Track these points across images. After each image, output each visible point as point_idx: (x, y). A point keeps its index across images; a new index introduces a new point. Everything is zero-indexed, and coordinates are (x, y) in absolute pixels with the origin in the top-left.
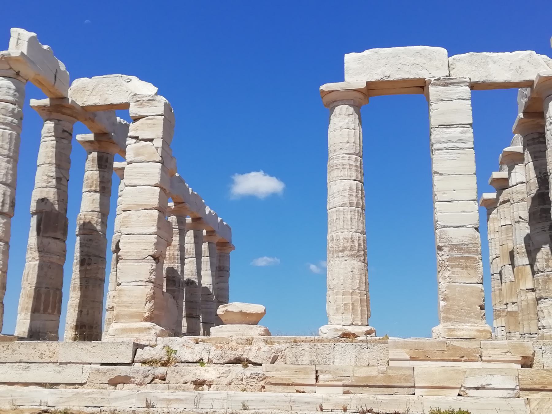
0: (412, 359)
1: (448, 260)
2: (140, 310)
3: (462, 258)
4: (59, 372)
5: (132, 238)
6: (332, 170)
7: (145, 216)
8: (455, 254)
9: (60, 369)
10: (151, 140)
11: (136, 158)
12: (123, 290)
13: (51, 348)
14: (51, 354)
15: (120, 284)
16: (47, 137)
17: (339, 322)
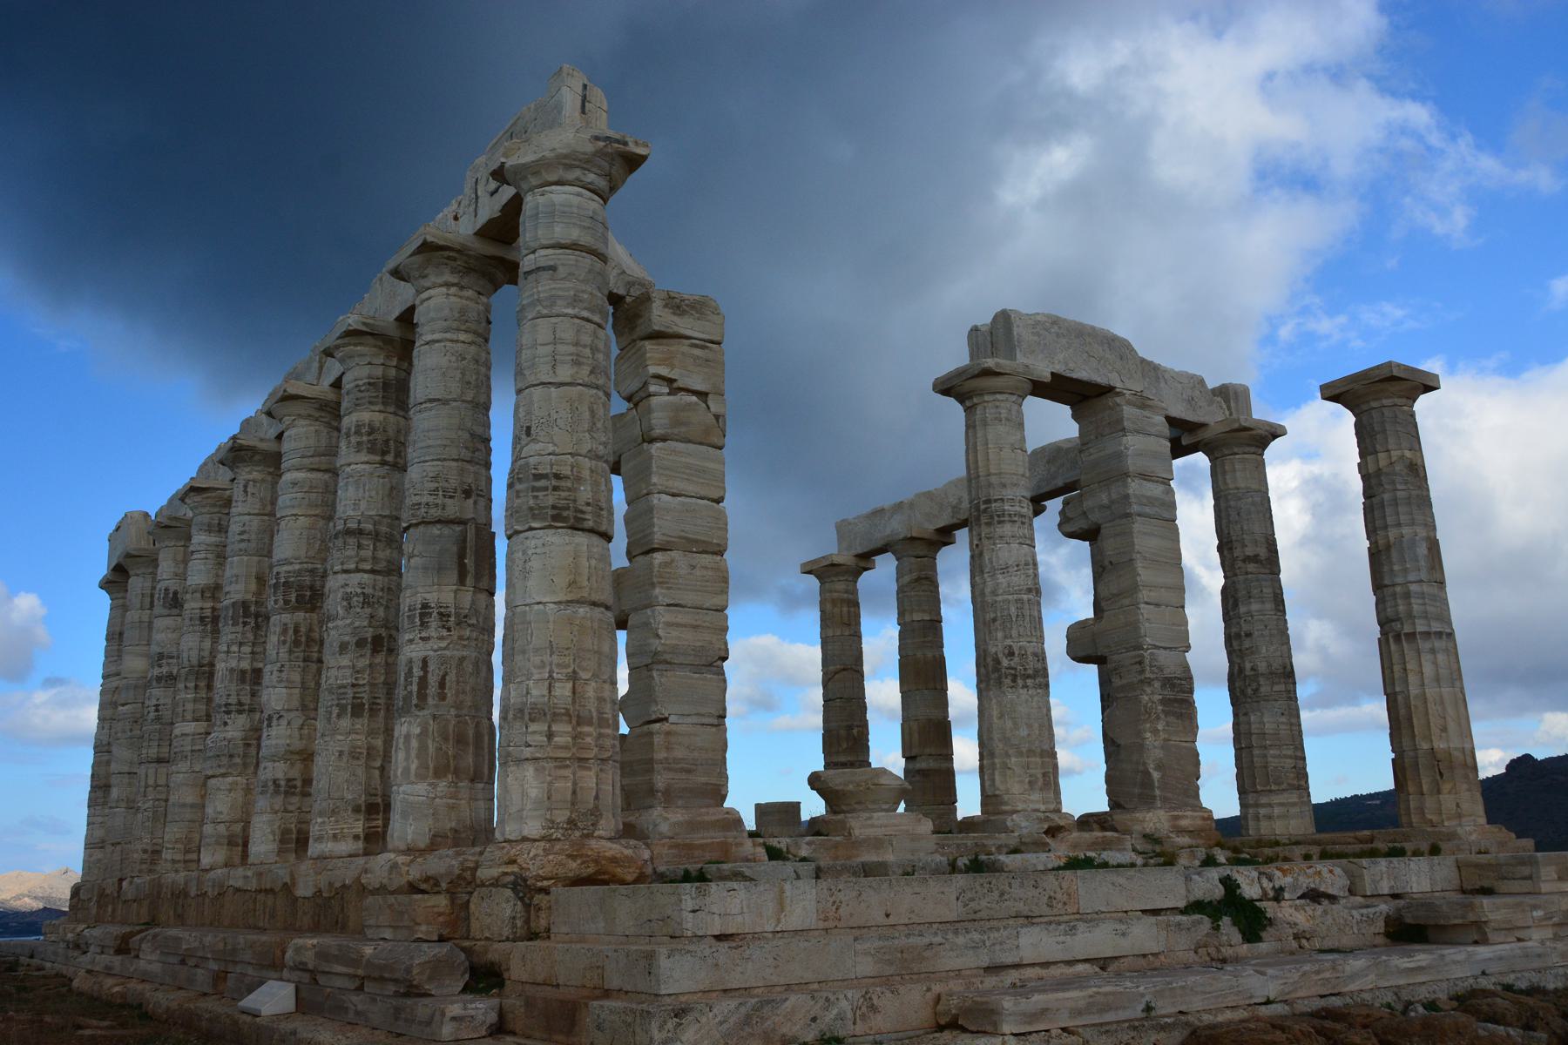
0: (1560, 879)
1: (1164, 702)
2: (714, 780)
3: (1176, 700)
4: (1123, 934)
5: (681, 617)
6: (1000, 522)
7: (706, 568)
8: (1169, 694)
9: (1123, 927)
10: (702, 395)
11: (676, 431)
12: (676, 733)
13: (1065, 885)
14: (1065, 898)
15: (666, 719)
16: (458, 330)
17: (1037, 806)
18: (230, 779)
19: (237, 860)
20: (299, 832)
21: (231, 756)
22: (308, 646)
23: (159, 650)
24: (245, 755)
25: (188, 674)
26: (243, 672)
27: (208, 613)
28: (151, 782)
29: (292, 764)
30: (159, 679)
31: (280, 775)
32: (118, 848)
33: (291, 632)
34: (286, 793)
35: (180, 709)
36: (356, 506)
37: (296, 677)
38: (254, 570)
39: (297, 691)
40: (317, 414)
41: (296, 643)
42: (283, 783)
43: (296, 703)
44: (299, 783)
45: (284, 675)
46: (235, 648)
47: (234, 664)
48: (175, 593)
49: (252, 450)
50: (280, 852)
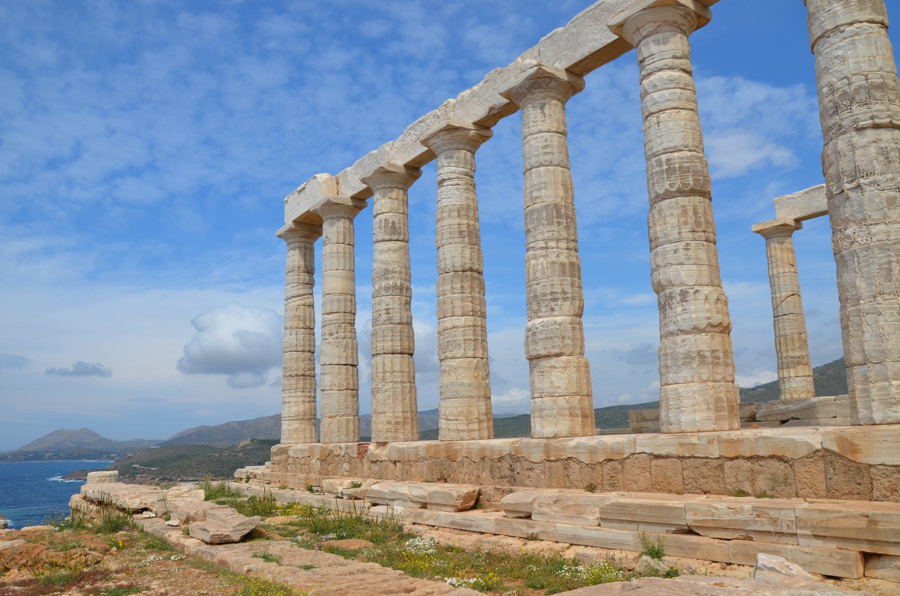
18: (564, 358)
19: (578, 429)
20: (727, 398)
21: (563, 338)
22: (707, 228)
23: (384, 267)
24: (574, 338)
25: (453, 277)
26: (563, 265)
27: (464, 228)
28: (388, 369)
29: (713, 336)
30: (387, 289)
31: (703, 347)
32: (335, 420)
33: (691, 213)
34: (713, 363)
35: (448, 306)
36: (872, 59)
37: (703, 255)
38: (560, 179)
39: (705, 268)
40: (680, 20)
41: (697, 223)
42: (708, 354)
43: (706, 280)
44: (721, 356)
45: (691, 253)
46: (552, 244)
47: (553, 258)
48: (393, 223)
49: (551, 77)
50: (718, 419)
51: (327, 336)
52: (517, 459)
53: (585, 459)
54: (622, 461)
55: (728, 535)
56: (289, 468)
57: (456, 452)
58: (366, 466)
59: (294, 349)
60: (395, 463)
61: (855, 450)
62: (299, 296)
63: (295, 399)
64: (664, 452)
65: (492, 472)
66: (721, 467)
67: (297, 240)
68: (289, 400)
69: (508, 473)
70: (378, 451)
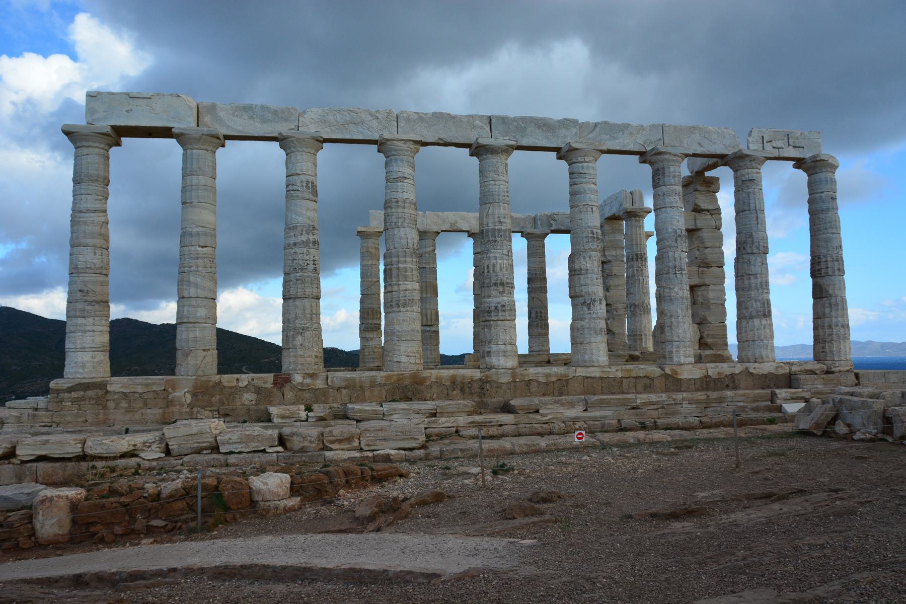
23: (310, 223)
51: (200, 269)
52: (488, 382)
53: (541, 379)
54: (567, 381)
55: (655, 407)
56: (111, 405)
57: (424, 380)
58: (289, 395)
59: (99, 271)
60: (338, 389)
61: (677, 373)
62: (95, 211)
63: (100, 328)
64: (593, 375)
65: (462, 390)
66: (622, 383)
67: (102, 146)
68: (95, 328)
69: (477, 390)
70: (308, 381)
